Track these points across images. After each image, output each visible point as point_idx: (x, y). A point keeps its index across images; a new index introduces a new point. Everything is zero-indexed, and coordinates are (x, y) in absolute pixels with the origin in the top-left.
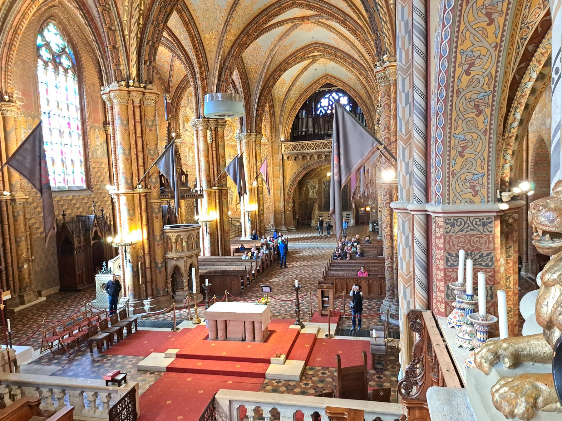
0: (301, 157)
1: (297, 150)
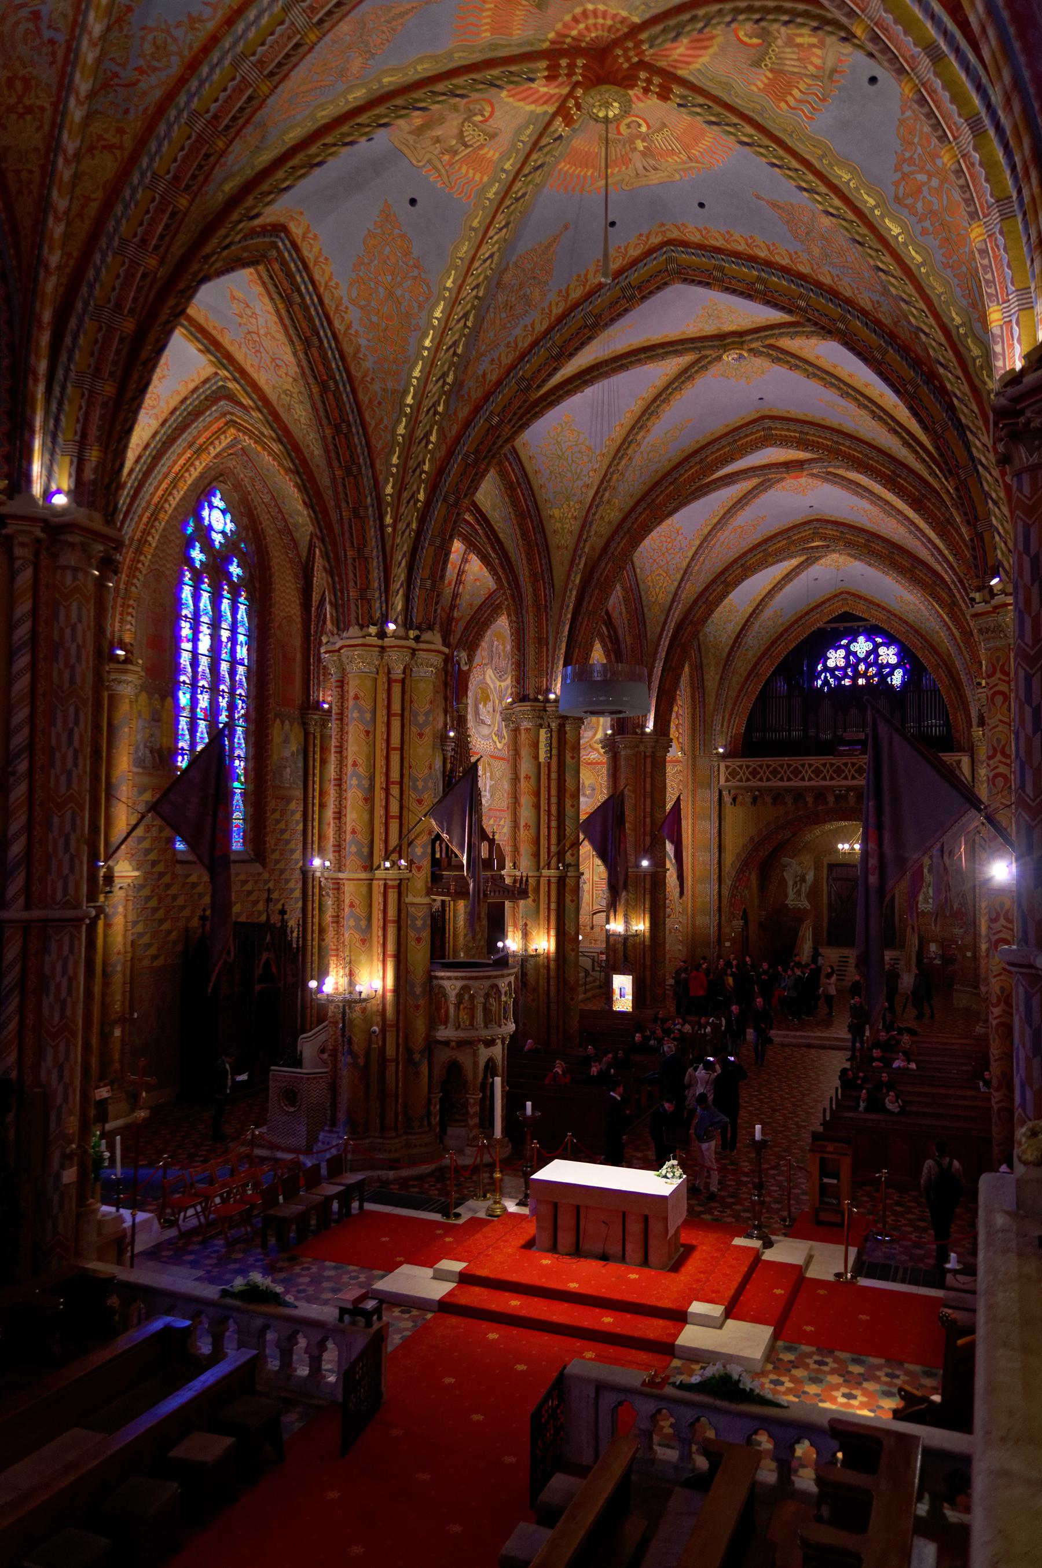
0: (768, 799)
1: (761, 780)
